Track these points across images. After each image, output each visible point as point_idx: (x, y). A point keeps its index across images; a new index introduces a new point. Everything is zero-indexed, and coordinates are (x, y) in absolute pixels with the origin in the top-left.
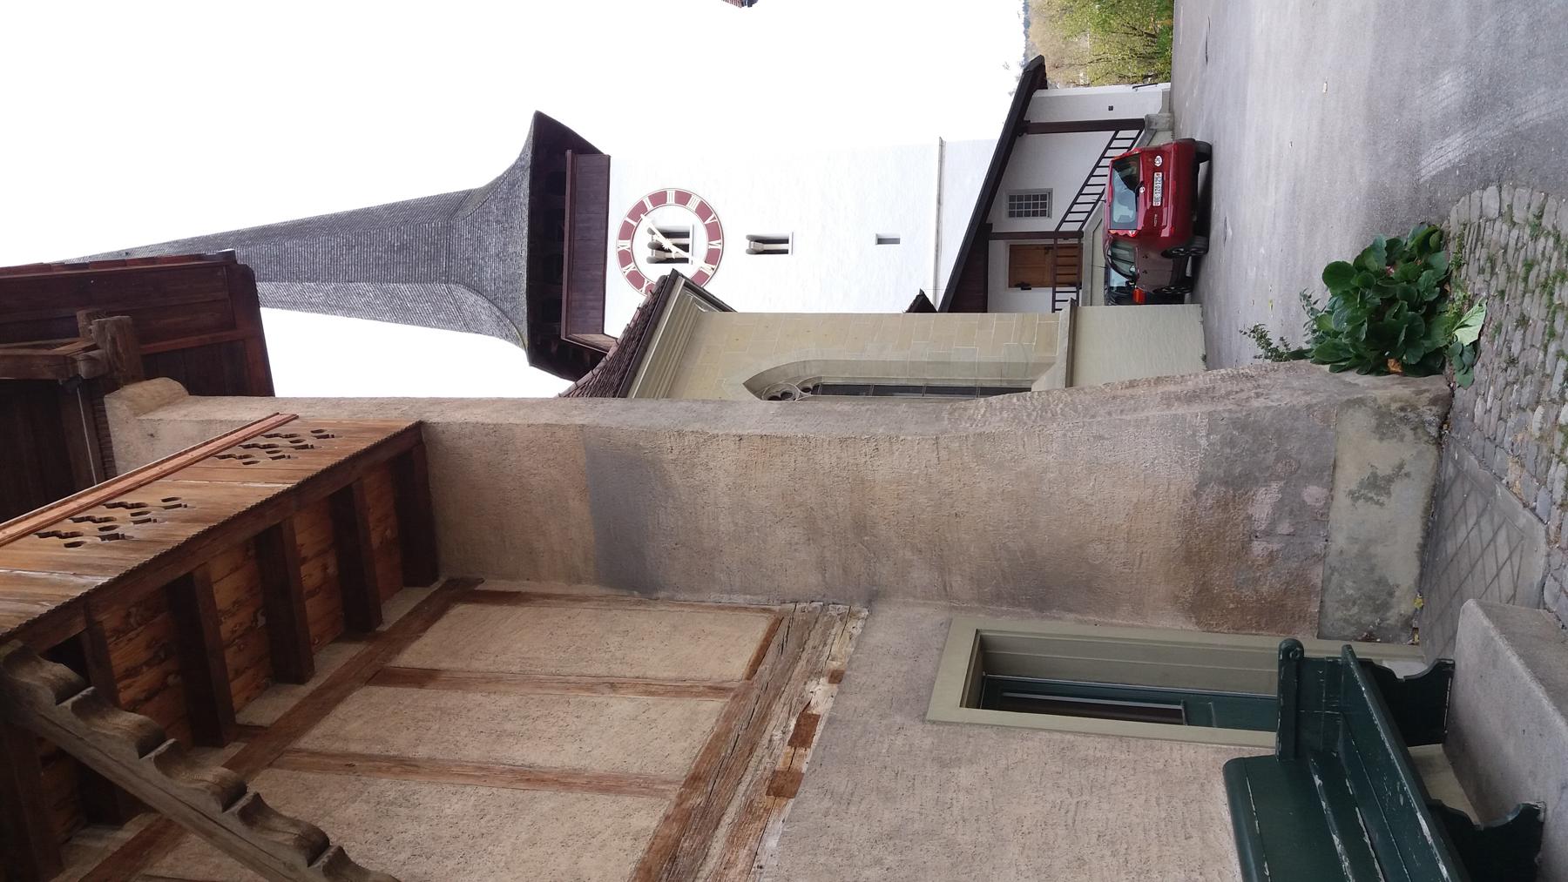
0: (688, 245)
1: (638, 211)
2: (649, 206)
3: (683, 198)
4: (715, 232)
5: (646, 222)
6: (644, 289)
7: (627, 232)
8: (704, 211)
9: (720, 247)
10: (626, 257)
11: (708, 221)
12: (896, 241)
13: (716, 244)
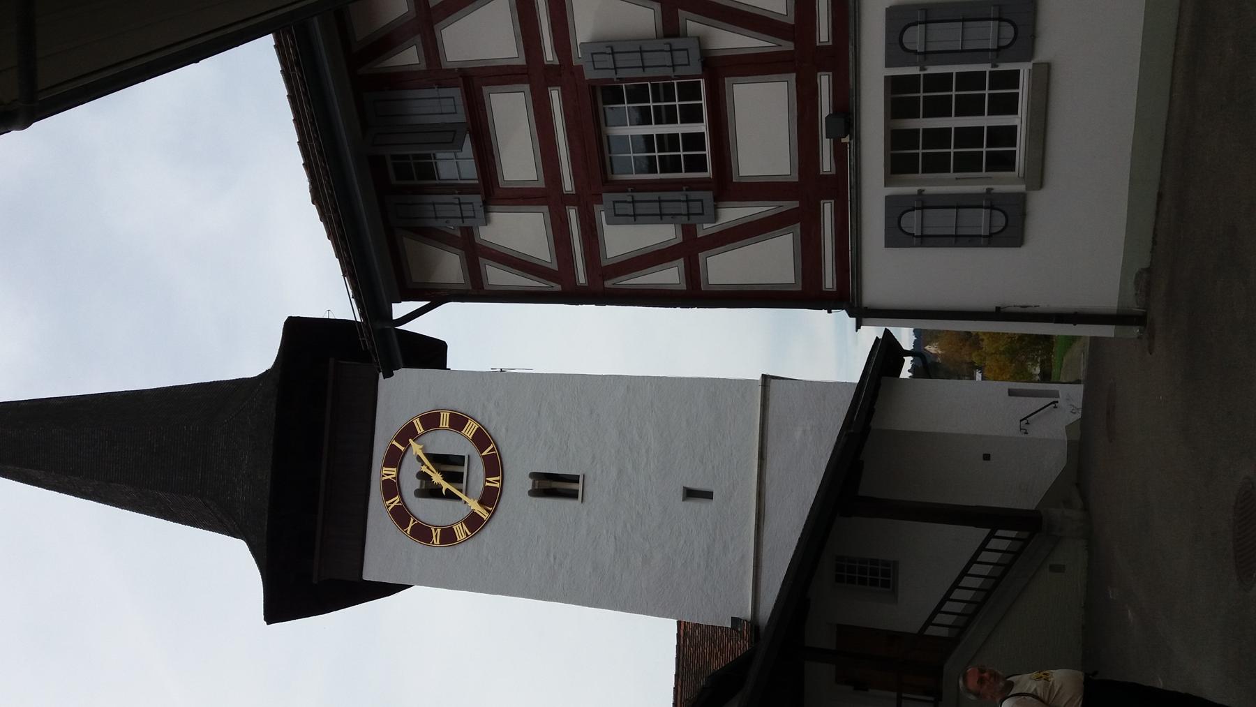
0: (463, 473)
1: (407, 434)
2: (420, 429)
3: (458, 422)
4: (493, 466)
6: (409, 528)
7: (394, 458)
8: (481, 439)
9: (497, 485)
10: (391, 489)
11: (485, 453)
12: (708, 495)
13: (494, 482)
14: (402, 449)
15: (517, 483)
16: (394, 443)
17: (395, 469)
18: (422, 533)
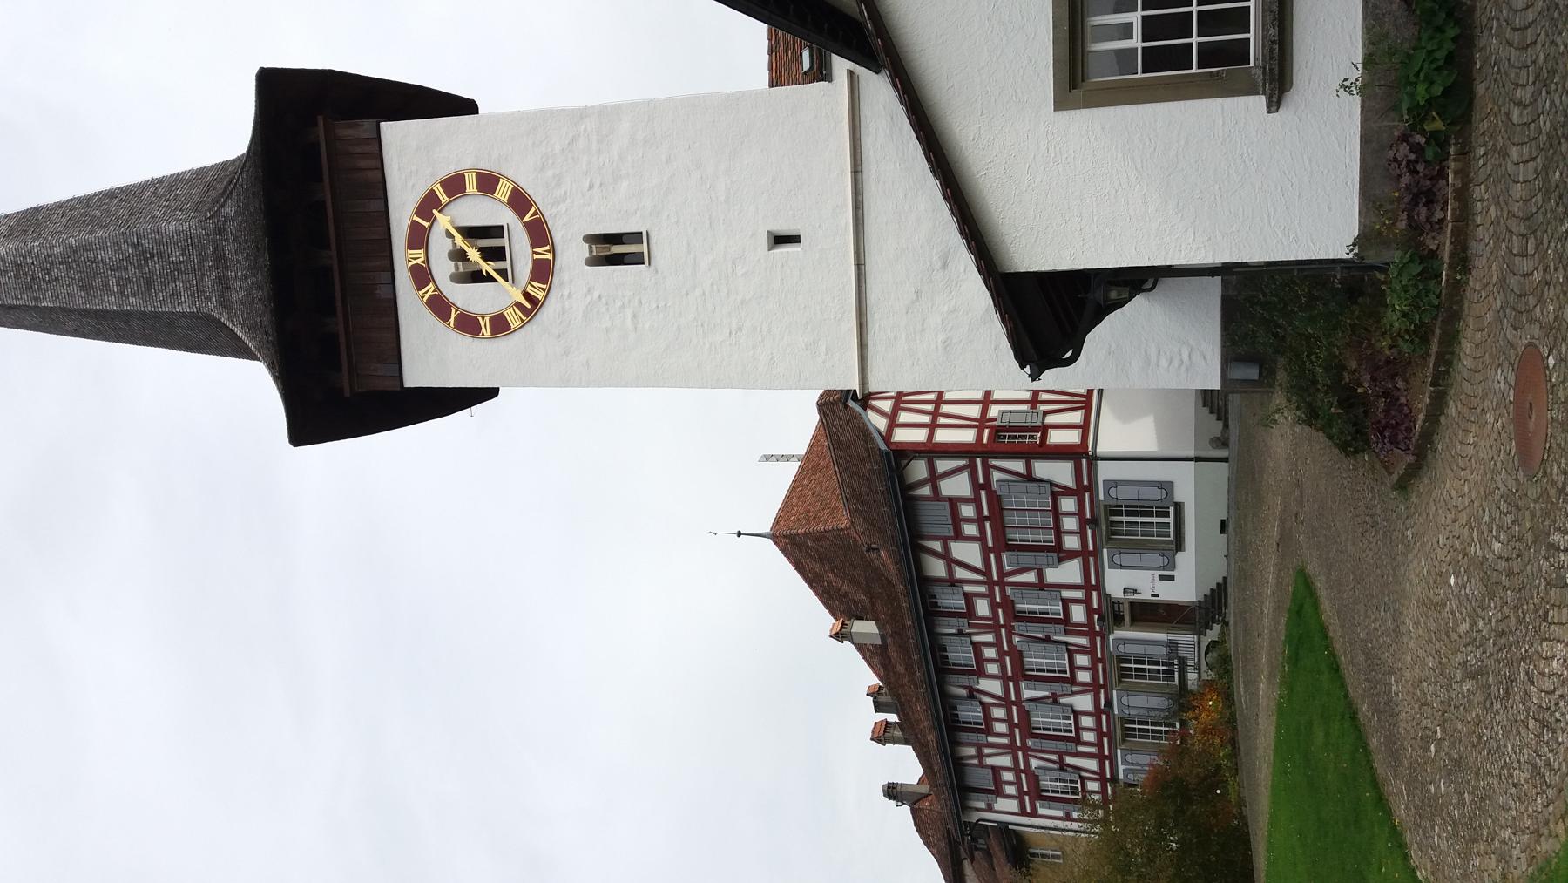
0: (503, 248)
2: (444, 199)
3: (488, 183)
4: (539, 233)
5: (443, 221)
6: (452, 320)
7: (418, 238)
8: (519, 201)
9: (549, 256)
10: (422, 275)
11: (527, 219)
13: (543, 253)
14: (426, 224)
15: (571, 253)
16: (416, 218)
17: (422, 251)
18: (468, 324)
